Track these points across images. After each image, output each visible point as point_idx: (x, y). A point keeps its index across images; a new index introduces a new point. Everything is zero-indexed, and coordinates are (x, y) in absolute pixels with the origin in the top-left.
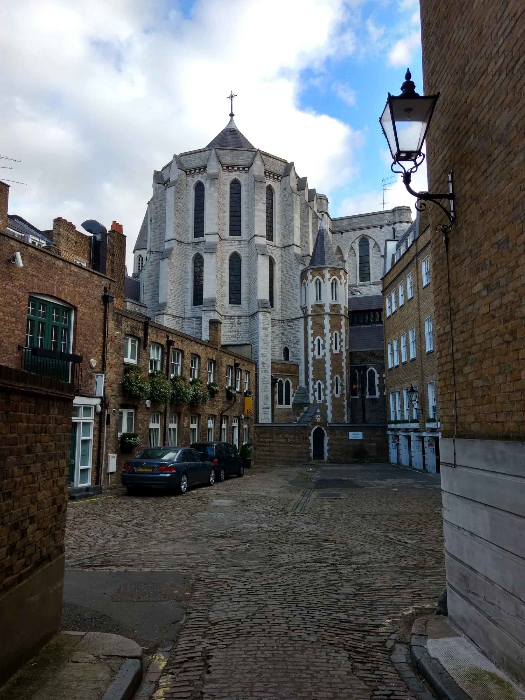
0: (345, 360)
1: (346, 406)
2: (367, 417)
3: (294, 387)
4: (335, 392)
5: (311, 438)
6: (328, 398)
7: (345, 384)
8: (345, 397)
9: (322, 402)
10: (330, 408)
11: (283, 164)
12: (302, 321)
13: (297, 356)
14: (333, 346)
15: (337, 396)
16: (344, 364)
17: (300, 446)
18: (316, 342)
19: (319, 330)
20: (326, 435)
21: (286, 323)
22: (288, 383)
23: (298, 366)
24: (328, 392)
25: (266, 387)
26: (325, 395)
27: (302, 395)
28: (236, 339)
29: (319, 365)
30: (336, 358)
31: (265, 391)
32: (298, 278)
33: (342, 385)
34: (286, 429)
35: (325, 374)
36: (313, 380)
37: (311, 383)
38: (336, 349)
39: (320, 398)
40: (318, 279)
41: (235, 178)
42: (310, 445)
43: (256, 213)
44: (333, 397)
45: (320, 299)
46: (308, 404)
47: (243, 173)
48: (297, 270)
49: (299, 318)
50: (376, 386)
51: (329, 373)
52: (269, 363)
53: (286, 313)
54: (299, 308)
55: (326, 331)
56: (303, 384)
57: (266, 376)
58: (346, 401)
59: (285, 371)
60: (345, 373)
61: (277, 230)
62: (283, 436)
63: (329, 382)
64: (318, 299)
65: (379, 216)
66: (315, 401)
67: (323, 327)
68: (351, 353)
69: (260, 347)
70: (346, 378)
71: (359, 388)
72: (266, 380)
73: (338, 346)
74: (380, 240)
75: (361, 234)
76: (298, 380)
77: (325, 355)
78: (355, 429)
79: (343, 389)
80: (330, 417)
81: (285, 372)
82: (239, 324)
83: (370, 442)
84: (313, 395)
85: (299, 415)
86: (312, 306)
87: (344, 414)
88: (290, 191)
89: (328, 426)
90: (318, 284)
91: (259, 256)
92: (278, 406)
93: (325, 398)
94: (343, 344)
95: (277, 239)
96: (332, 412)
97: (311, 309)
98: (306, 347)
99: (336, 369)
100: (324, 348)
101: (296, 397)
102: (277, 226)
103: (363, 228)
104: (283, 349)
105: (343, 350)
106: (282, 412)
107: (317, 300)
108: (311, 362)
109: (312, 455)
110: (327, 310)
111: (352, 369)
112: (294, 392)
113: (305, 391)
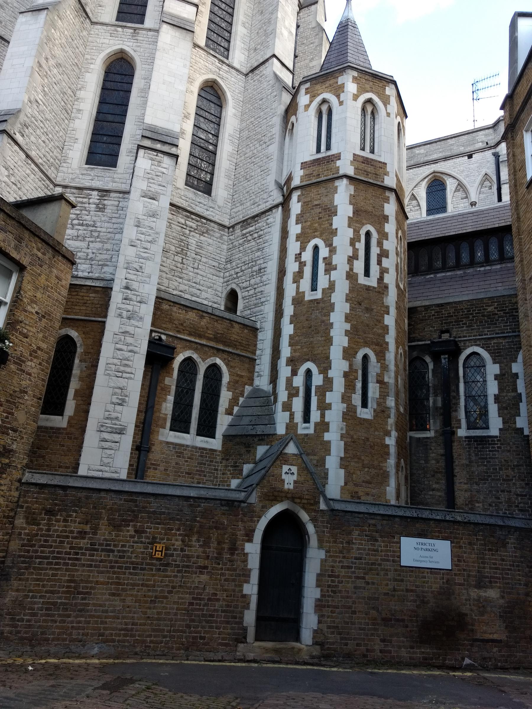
0: (393, 311)
1: (393, 450)
2: (461, 497)
3: (236, 385)
4: (357, 399)
5: (253, 549)
6: (334, 416)
7: (392, 381)
8: (391, 421)
9: (311, 431)
13: (256, 305)
14: (359, 266)
15: (366, 414)
16: (390, 320)
17: (204, 578)
18: (307, 256)
19: (318, 222)
20: (313, 541)
21: (238, 231)
22: (213, 372)
23: (254, 330)
24: (334, 397)
25: (125, 362)
26: (324, 407)
27: (257, 411)
28: (84, 245)
29: (312, 318)
30: (365, 301)
31: (120, 374)
32: (277, 121)
33: (380, 381)
34: (154, 505)
35: (329, 341)
37: (284, 371)
38: (367, 273)
39: (306, 418)
40: (324, 101)
42: (246, 575)
44: (349, 415)
45: (328, 148)
46: (267, 438)
48: (275, 105)
49: (270, 209)
50: (491, 400)
52: (149, 291)
53: (240, 208)
54: (272, 186)
55: (340, 221)
56: (262, 382)
57: (130, 329)
58: (394, 434)
59: (210, 333)
60: (392, 347)
61: (238, 38)
62: (139, 532)
63: (339, 366)
65: (465, 137)
66: (291, 426)
67: (332, 211)
68: (412, 311)
69: (125, 241)
70: (396, 365)
71: (436, 408)
72: (129, 340)
73: (374, 269)
74: (467, 176)
75: (432, 171)
76: (252, 371)
77: (332, 286)
78: (423, 529)
79: (384, 395)
80: (335, 482)
81: (209, 339)
82: (101, 208)
83: (479, 585)
84: (287, 407)
85: (237, 472)
86: (304, 165)
87: (385, 476)
89: (323, 506)
91: (165, 27)
92: (168, 436)
93: (323, 416)
94: (389, 263)
95: (239, 56)
96: (344, 463)
97: (301, 173)
98: (282, 272)
100: (330, 267)
101: (239, 416)
102: (240, 31)
103: (435, 161)
104: (224, 295)
105: (390, 279)
106: (179, 454)
107: (318, 150)
108: (289, 309)
109: (250, 617)
110: (346, 167)
111: (415, 354)
112: (234, 402)
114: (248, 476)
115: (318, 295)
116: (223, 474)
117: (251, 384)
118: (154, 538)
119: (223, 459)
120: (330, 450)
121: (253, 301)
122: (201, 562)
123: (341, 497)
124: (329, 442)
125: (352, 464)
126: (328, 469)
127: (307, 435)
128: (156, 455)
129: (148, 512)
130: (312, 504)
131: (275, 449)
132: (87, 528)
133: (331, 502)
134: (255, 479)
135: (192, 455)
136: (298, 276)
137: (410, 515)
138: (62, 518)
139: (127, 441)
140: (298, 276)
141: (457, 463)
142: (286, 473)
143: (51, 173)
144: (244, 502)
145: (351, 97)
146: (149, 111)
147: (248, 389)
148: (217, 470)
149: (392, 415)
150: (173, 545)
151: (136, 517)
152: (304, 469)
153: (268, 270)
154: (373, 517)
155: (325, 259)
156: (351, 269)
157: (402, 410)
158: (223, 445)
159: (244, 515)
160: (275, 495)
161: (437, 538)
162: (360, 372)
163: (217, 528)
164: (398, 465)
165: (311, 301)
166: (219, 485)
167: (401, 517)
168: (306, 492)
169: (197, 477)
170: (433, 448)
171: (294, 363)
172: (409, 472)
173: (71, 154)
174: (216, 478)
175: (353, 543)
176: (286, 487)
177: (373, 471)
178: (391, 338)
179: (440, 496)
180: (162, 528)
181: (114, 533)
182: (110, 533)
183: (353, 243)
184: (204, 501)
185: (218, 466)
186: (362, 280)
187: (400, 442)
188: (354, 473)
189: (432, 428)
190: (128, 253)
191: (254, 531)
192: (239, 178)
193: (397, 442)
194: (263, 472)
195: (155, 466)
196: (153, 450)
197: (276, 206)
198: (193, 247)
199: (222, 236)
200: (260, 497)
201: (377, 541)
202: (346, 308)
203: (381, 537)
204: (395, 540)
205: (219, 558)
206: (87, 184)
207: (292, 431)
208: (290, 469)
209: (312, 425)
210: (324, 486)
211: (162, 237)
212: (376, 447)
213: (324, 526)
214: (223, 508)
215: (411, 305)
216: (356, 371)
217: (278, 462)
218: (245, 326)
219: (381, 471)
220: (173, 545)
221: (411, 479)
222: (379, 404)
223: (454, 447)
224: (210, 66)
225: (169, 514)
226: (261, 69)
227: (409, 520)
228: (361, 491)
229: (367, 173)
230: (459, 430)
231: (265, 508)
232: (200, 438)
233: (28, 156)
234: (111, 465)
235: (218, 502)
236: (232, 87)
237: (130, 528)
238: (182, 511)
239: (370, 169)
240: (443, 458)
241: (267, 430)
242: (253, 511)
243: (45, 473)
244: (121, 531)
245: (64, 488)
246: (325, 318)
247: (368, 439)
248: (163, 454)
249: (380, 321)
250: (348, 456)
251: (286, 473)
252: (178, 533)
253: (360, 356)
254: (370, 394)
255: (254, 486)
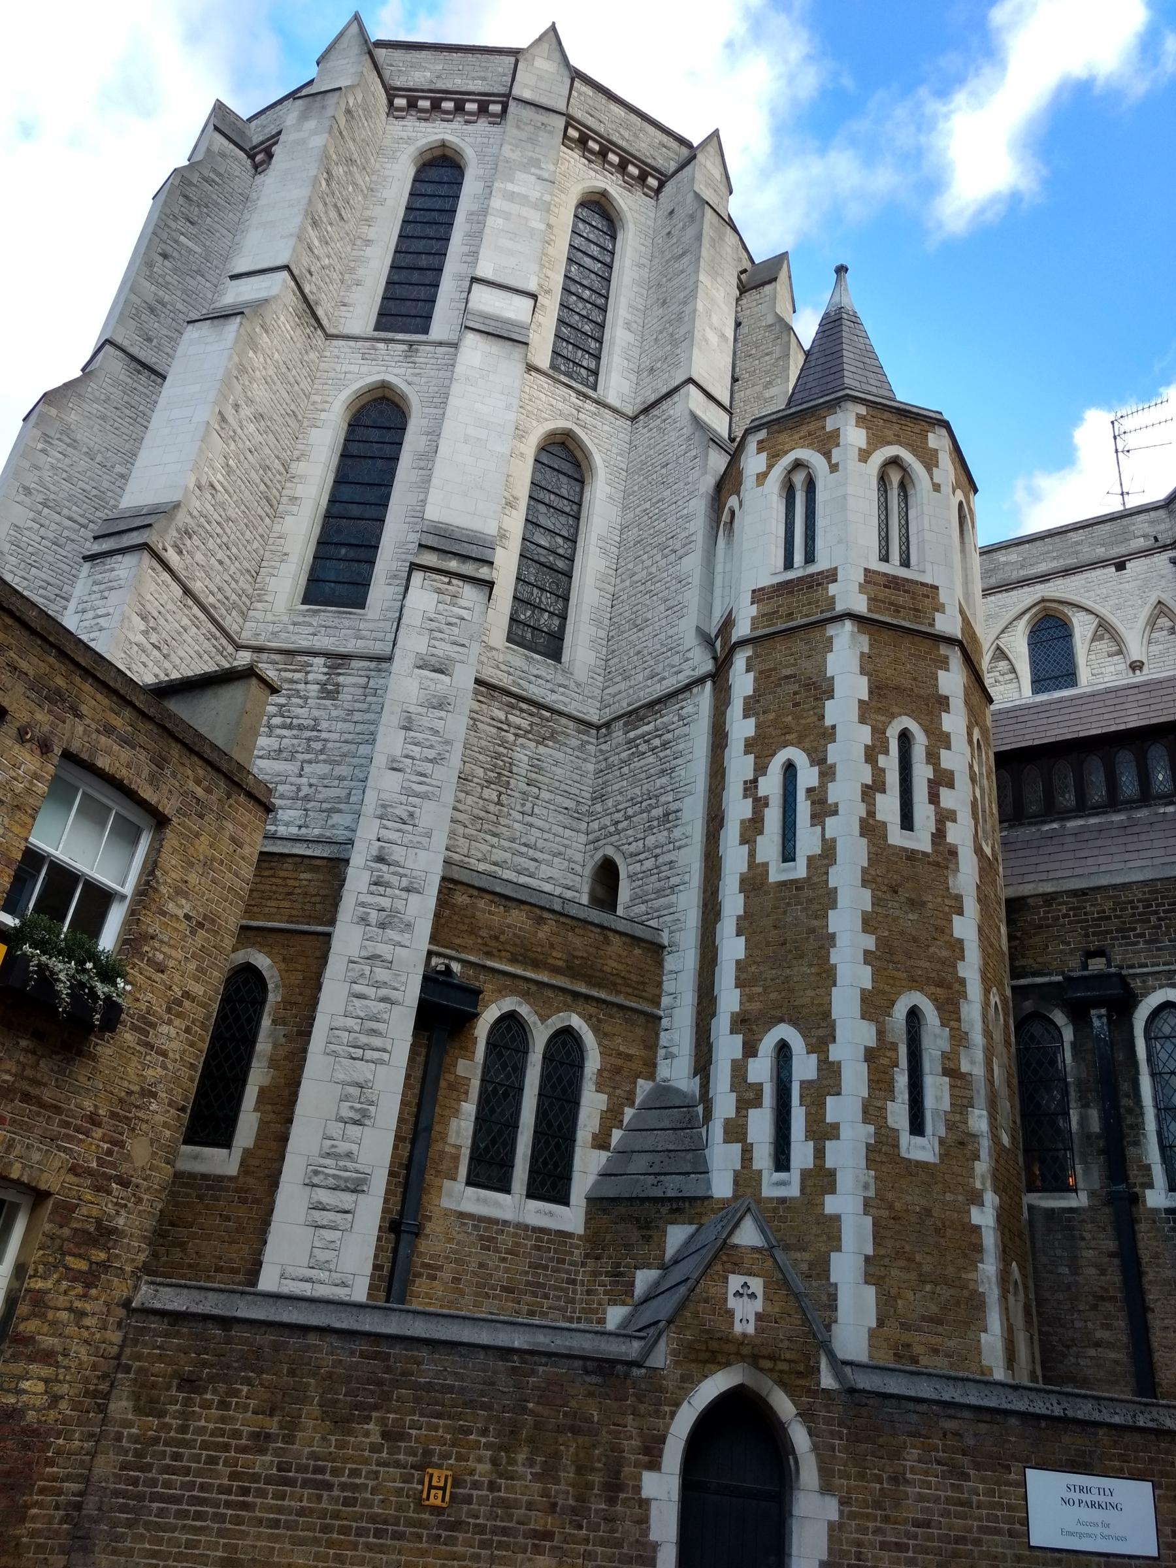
0: (971, 905)
1: (989, 1239)
3: (616, 1078)
4: (898, 1113)
5: (662, 1488)
6: (847, 1155)
7: (978, 1071)
8: (982, 1167)
10: (856, 1238)
11: (674, 144)
12: (706, 693)
13: (659, 893)
14: (888, 806)
15: (921, 1150)
16: (966, 928)
18: (771, 786)
19: (793, 711)
21: (618, 735)
22: (565, 1046)
23: (656, 950)
24: (844, 1109)
25: (371, 1025)
26: (822, 1132)
27: (664, 1141)
28: (291, 768)
29: (788, 923)
30: (907, 885)
31: (359, 1052)
32: (699, 507)
33: (951, 1072)
34: (430, 1368)
35: (828, 976)
36: (741, 1022)
37: (727, 1046)
38: (907, 822)
39: (782, 1161)
40: (798, 465)
41: (443, 145)
43: (496, 203)
44: (881, 1151)
45: (810, 558)
47: (482, 124)
48: (694, 475)
49: (688, 688)
51: (852, 972)
52: (428, 866)
53: (622, 686)
54: (691, 640)
55: (843, 709)
56: (677, 1071)
57: (384, 950)
58: (991, 1198)
59: (558, 957)
60: (974, 989)
61: (617, 350)
62: (391, 1436)
63: (853, 1036)
64: (799, 557)
65: (1107, 527)
66: (746, 1178)
67: (823, 689)
68: (1015, 906)
69: (380, 760)
70: (987, 1034)
72: (381, 974)
73: (923, 812)
75: (1037, 597)
76: (651, 1044)
77: (829, 852)
79: (961, 1105)
81: (555, 970)
82: (330, 692)
84: (736, 1131)
85: (622, 1289)
86: (758, 595)
87: (977, 1304)
88: (690, 203)
89: (827, 1380)
90: (801, 493)
91: (470, 337)
92: (460, 1197)
93: (820, 1154)
94: (955, 799)
95: (618, 383)
97: (753, 610)
98: (715, 819)
99: (909, 950)
100: (822, 810)
101: (624, 1153)
103: (1044, 578)
104: (588, 871)
105: (960, 834)
106: (488, 1243)
107: (789, 564)
108: (733, 903)
110: (849, 595)
111: (1028, 1005)
112: (611, 1118)
113: (685, 1116)
114: (647, 1299)
115: (799, 870)
116: (589, 1292)
117: (651, 1076)
118: (427, 1453)
119: (587, 1256)
120: (840, 1239)
121: (653, 883)
122: (540, 1521)
123: (871, 1357)
124: (837, 1218)
125: (894, 1272)
126: (836, 1284)
127: (783, 1200)
128: (434, 1243)
129: (416, 1386)
130: (800, 1375)
131: (709, 1234)
132: (273, 1425)
133: (848, 1370)
134: (663, 1308)
135: (517, 1244)
136: (752, 828)
137: (1044, 1411)
138: (217, 1399)
139: (370, 1210)
140: (752, 828)
141: (1150, 1276)
142: (738, 1294)
143: (231, 623)
144: (637, 1364)
145: (854, 454)
146: (434, 496)
147: (643, 1087)
148: (574, 1282)
149: (984, 1153)
150: (472, 1473)
151: (386, 1397)
152: (779, 1284)
153: (685, 816)
154: (951, 1412)
155: (810, 791)
156: (871, 813)
157: (1006, 1140)
158: (587, 1221)
159: (640, 1399)
160: (711, 1350)
161: (1118, 1474)
162: (903, 1050)
163: (575, 1430)
164: (1004, 1278)
165: (783, 884)
166: (579, 1318)
167: (1024, 1416)
168: (786, 1344)
169: (528, 1298)
170: (1087, 1236)
171: (748, 1025)
172: (1032, 1296)
173: (273, 584)
174: (573, 1301)
175: (907, 1482)
176: (738, 1328)
177: (945, 1292)
178: (970, 969)
179: (1116, 1362)
180: (445, 1426)
181: (333, 1438)
182: (324, 1439)
183: (871, 755)
184: (544, 1360)
185: (577, 1273)
186: (896, 837)
187: (1006, 1219)
188: (899, 1296)
189: (1081, 1185)
190: (385, 784)
191: (662, 1440)
192: (620, 623)
193: (999, 1219)
194: (683, 1289)
195: (433, 1271)
196: (427, 1231)
197: (700, 681)
198: (522, 768)
199: (584, 744)
200: (674, 1353)
201: (966, 1477)
202: (865, 899)
203: (978, 1466)
204: (1013, 1476)
205: (579, 1511)
206: (304, 643)
207: (749, 1191)
208: (745, 1285)
209: (795, 1176)
210: (828, 1328)
211: (458, 748)
212: (949, 1232)
213: (832, 1433)
214: (588, 1379)
215: (1012, 892)
216: (894, 1047)
217: (718, 1267)
218: (635, 940)
219: (966, 1293)
220: (472, 1473)
221: (1039, 1314)
222: (951, 1126)
223: (1140, 1236)
224: (560, 405)
225: (462, 1390)
226: (664, 407)
227: (1043, 1424)
228: (919, 1342)
229: (897, 609)
230: (1148, 1192)
231: (690, 1381)
232: (534, 1204)
233: (187, 591)
234: (332, 1267)
235: (578, 1363)
236: (604, 442)
237: (371, 1426)
238: (492, 1384)
239: (902, 599)
240: (1116, 1261)
241: (691, 1188)
242: (661, 1389)
243: (185, 1286)
244: (350, 1432)
245: (226, 1322)
246: (815, 923)
247: (928, 1212)
248: (450, 1240)
249: (944, 929)
250: (882, 1252)
251: (738, 1294)
252: (483, 1440)
253: (900, 1011)
254: (929, 1102)
255: (662, 1324)
